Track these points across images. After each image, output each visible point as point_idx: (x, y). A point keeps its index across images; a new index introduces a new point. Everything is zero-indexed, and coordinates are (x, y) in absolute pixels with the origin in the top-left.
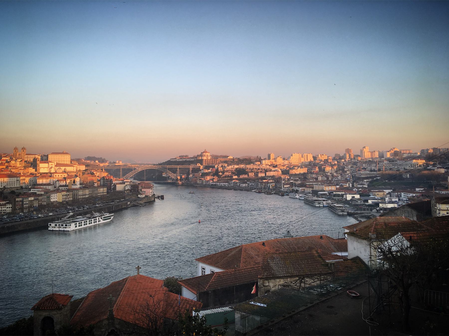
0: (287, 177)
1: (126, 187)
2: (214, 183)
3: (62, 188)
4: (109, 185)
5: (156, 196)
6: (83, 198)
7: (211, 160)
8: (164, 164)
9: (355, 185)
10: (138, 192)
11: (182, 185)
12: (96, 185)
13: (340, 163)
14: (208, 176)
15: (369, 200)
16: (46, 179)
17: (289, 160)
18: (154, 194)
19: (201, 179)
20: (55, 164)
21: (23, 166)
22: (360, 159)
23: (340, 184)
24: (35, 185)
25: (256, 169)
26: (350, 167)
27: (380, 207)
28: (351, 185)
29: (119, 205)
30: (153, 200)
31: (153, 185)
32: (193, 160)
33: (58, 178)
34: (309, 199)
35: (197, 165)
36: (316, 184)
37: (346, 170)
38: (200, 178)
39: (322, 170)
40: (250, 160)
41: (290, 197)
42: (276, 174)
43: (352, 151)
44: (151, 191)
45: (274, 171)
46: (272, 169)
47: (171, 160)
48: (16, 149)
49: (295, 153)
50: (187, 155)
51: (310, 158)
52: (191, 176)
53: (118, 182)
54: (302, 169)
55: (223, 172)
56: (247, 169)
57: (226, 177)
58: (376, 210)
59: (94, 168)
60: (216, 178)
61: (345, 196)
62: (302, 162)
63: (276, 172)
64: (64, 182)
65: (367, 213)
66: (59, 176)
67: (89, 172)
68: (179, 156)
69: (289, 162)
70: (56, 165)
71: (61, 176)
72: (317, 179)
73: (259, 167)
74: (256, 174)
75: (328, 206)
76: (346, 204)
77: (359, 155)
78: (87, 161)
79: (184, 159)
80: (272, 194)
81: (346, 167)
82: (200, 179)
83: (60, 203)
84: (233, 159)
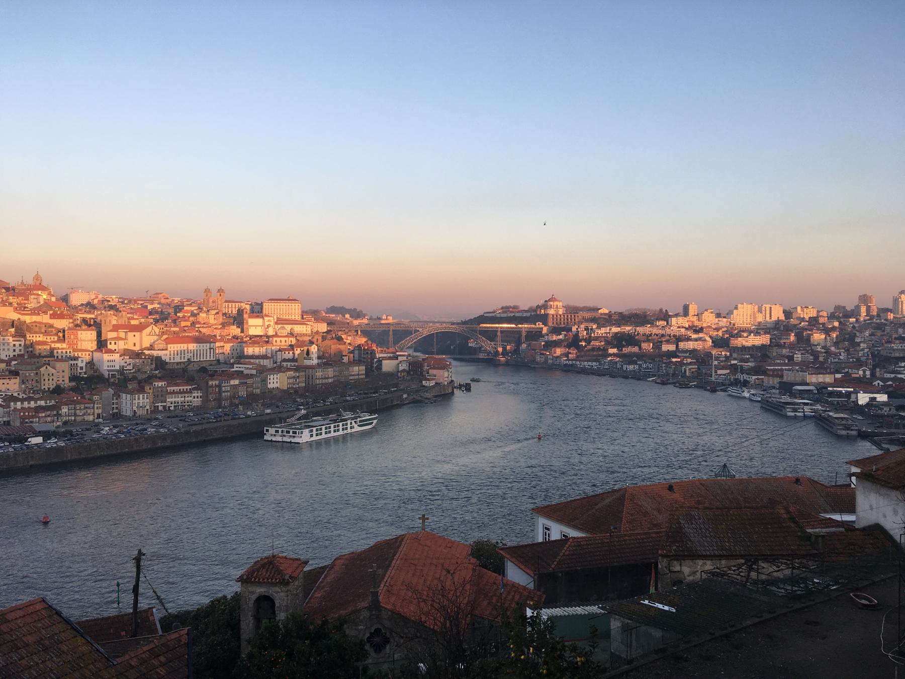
1: (400, 365)
3: (287, 365)
4: (369, 360)
5: (456, 385)
6: (322, 384)
8: (471, 321)
9: (878, 374)
10: (423, 376)
11: (507, 364)
12: (345, 359)
13: (846, 325)
14: (559, 347)
16: (259, 347)
17: (730, 318)
18: (452, 381)
20: (274, 319)
21: (220, 323)
22: (892, 317)
23: (843, 371)
24: (241, 357)
26: (867, 333)
28: (868, 373)
29: (387, 399)
30: (450, 391)
31: (450, 363)
32: (528, 314)
33: (280, 346)
35: (536, 325)
36: (789, 370)
37: (858, 340)
38: (542, 352)
39: (803, 340)
41: (730, 395)
43: (874, 299)
44: (446, 374)
45: (696, 340)
47: (485, 315)
48: (207, 291)
49: (743, 304)
51: (778, 314)
52: (524, 346)
53: (385, 355)
54: (759, 337)
56: (638, 335)
57: (593, 349)
59: (343, 327)
60: (575, 352)
61: (853, 397)
62: (760, 323)
64: (291, 352)
66: (281, 341)
67: (334, 336)
68: (500, 307)
69: (730, 323)
71: (286, 341)
72: (791, 358)
73: (661, 332)
74: (658, 345)
75: (814, 416)
76: (855, 414)
77: (890, 307)
78: (331, 315)
79: (511, 312)
81: (858, 334)
82: (543, 354)
83: (283, 391)
84: (610, 315)
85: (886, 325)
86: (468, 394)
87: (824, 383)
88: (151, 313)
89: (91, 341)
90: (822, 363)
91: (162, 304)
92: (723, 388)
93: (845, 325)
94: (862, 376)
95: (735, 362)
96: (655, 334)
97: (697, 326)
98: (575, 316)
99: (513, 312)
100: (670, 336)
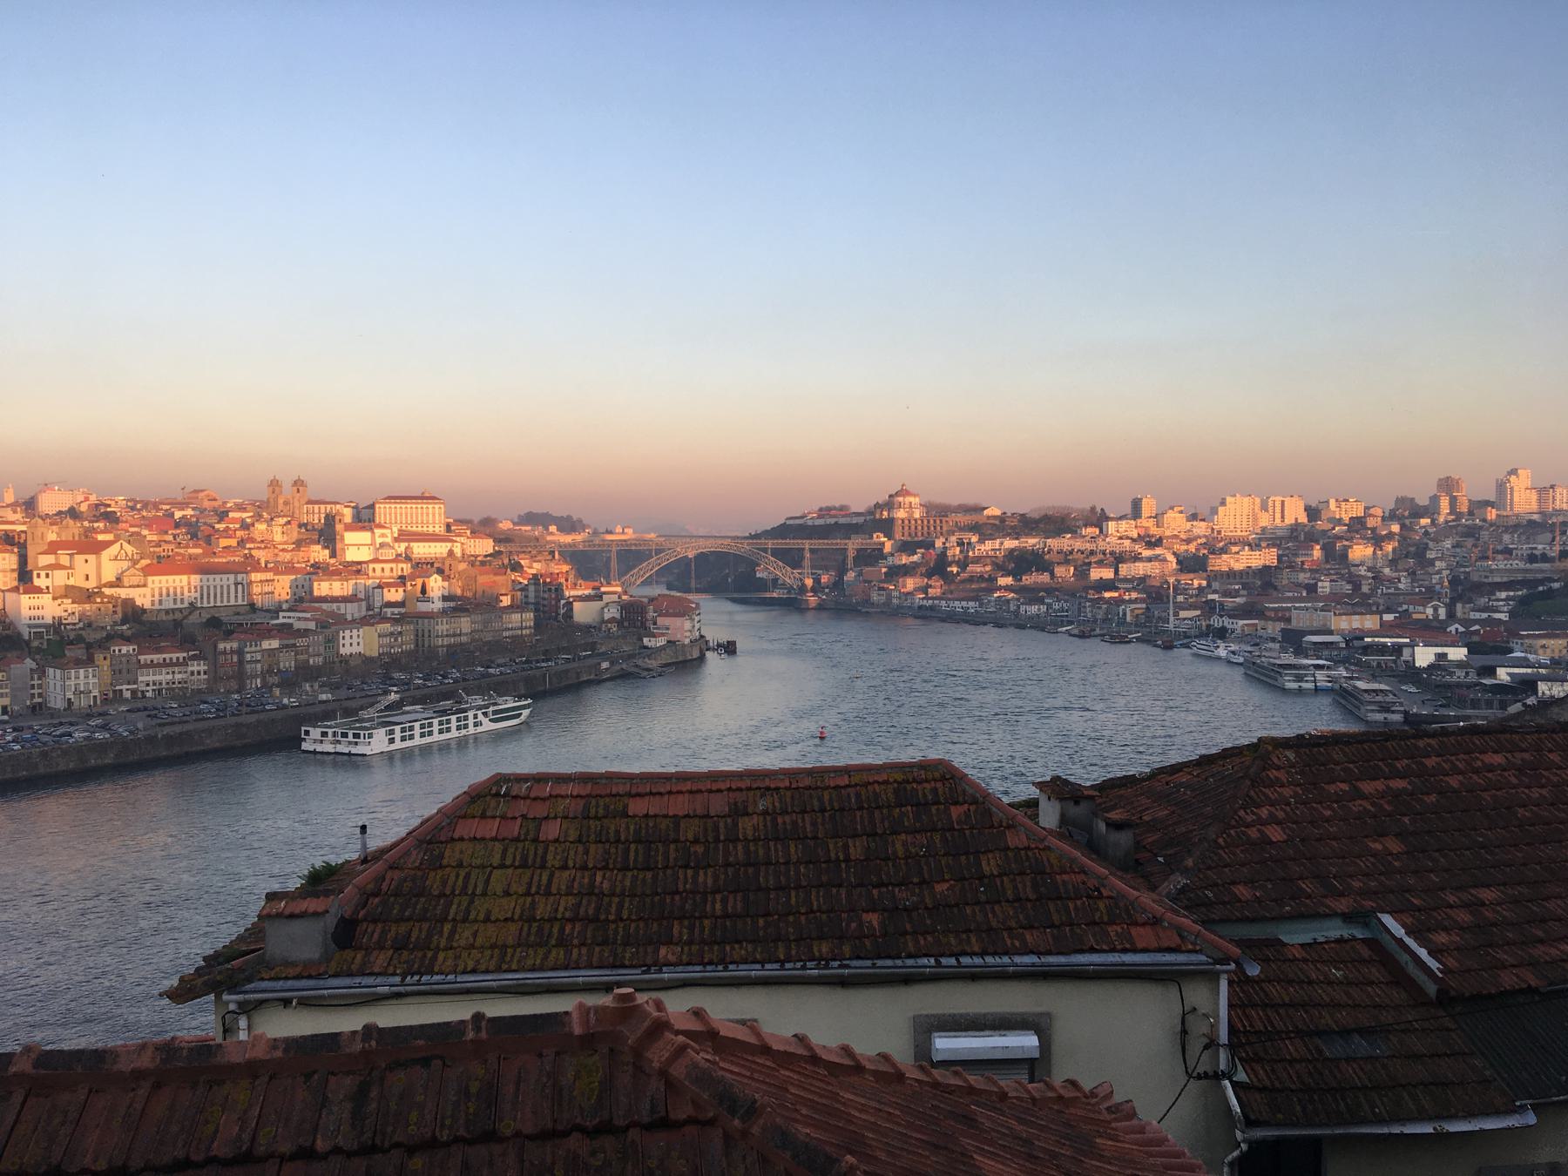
1: (606, 610)
2: (930, 602)
5: (711, 644)
7: (922, 521)
9: (1459, 614)
11: (821, 608)
13: (1414, 530)
14: (911, 576)
16: (340, 580)
17: (1213, 521)
18: (702, 637)
21: (294, 540)
22: (1494, 517)
23: (1400, 609)
24: (302, 599)
25: (1083, 553)
26: (1448, 544)
27: (1540, 694)
28: (1442, 613)
30: (696, 654)
31: (697, 604)
32: (861, 520)
33: (381, 578)
34: (1263, 659)
35: (872, 537)
37: (1431, 555)
38: (881, 585)
39: (1336, 557)
42: (1157, 571)
44: (688, 625)
45: (1150, 560)
46: (1140, 554)
47: (788, 522)
48: (274, 484)
49: (1235, 496)
50: (843, 503)
51: (1295, 513)
52: (850, 576)
53: (580, 593)
54: (1258, 553)
55: (963, 564)
56: (1049, 552)
57: (971, 580)
58: (1524, 705)
61: (1406, 652)
62: (1264, 529)
63: (1157, 563)
64: (401, 590)
66: (383, 569)
68: (817, 509)
69: (1213, 529)
70: (396, 535)
72: (1312, 589)
73: (1089, 546)
74: (1082, 571)
78: (523, 528)
79: (832, 517)
80: (1130, 642)
81: (1431, 544)
82: (881, 589)
84: (1002, 519)
85: (1481, 528)
87: (1361, 630)
88: (177, 525)
89: (13, 570)
91: (203, 511)
92: (1185, 641)
93: (1411, 529)
95: (1215, 597)
96: (1079, 550)
98: (941, 521)
99: (834, 516)
100: (1104, 554)
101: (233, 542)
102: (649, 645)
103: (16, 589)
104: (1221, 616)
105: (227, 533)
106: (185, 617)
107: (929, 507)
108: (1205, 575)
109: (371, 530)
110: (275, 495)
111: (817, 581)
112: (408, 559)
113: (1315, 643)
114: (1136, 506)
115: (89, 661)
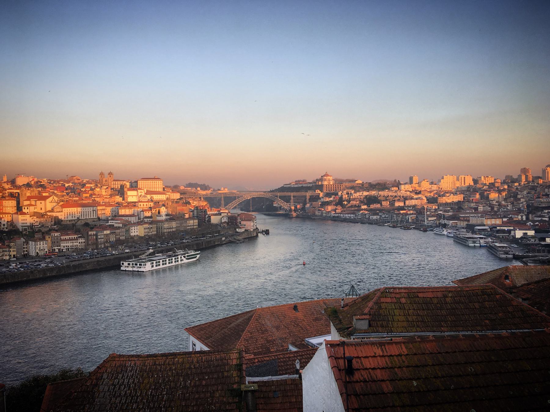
0: (434, 207)
1: (223, 219)
2: (337, 215)
4: (203, 216)
5: (260, 230)
9: (530, 218)
10: (237, 225)
12: (187, 216)
14: (330, 205)
15: (546, 238)
16: (129, 209)
18: (257, 228)
19: (321, 209)
21: (109, 194)
22: (542, 182)
23: (509, 217)
24: (116, 216)
26: (525, 192)
30: (255, 234)
32: (311, 185)
34: (461, 235)
35: (315, 192)
36: (473, 217)
37: (519, 197)
39: (485, 198)
40: (385, 185)
42: (419, 203)
43: (530, 171)
44: (252, 224)
45: (417, 199)
46: (413, 197)
48: (102, 174)
49: (447, 175)
50: (305, 179)
51: (469, 181)
52: (308, 205)
53: (213, 213)
54: (456, 196)
55: (349, 201)
57: (352, 206)
59: (191, 196)
60: (340, 208)
61: (512, 233)
62: (458, 187)
63: (419, 200)
64: (150, 212)
65: (542, 256)
66: (143, 205)
69: (439, 188)
70: (146, 192)
71: (147, 205)
72: (476, 209)
73: (394, 194)
74: (392, 203)
75: (486, 246)
78: (188, 189)
81: (519, 193)
82: (320, 210)
84: (362, 184)
85: (537, 186)
86: (268, 237)
88: (67, 189)
89: (15, 206)
90: (496, 212)
91: (75, 183)
93: (511, 187)
94: (520, 219)
97: (417, 190)
98: (340, 185)
99: (302, 184)
100: (400, 197)
101: (88, 195)
102: (239, 231)
103: (16, 213)
104: (444, 220)
105: (85, 192)
106: (76, 223)
107: (335, 180)
108: (437, 204)
109: (137, 190)
110: (102, 178)
111: (296, 207)
112: (152, 201)
113: (479, 229)
114: (411, 179)
115: (43, 239)
